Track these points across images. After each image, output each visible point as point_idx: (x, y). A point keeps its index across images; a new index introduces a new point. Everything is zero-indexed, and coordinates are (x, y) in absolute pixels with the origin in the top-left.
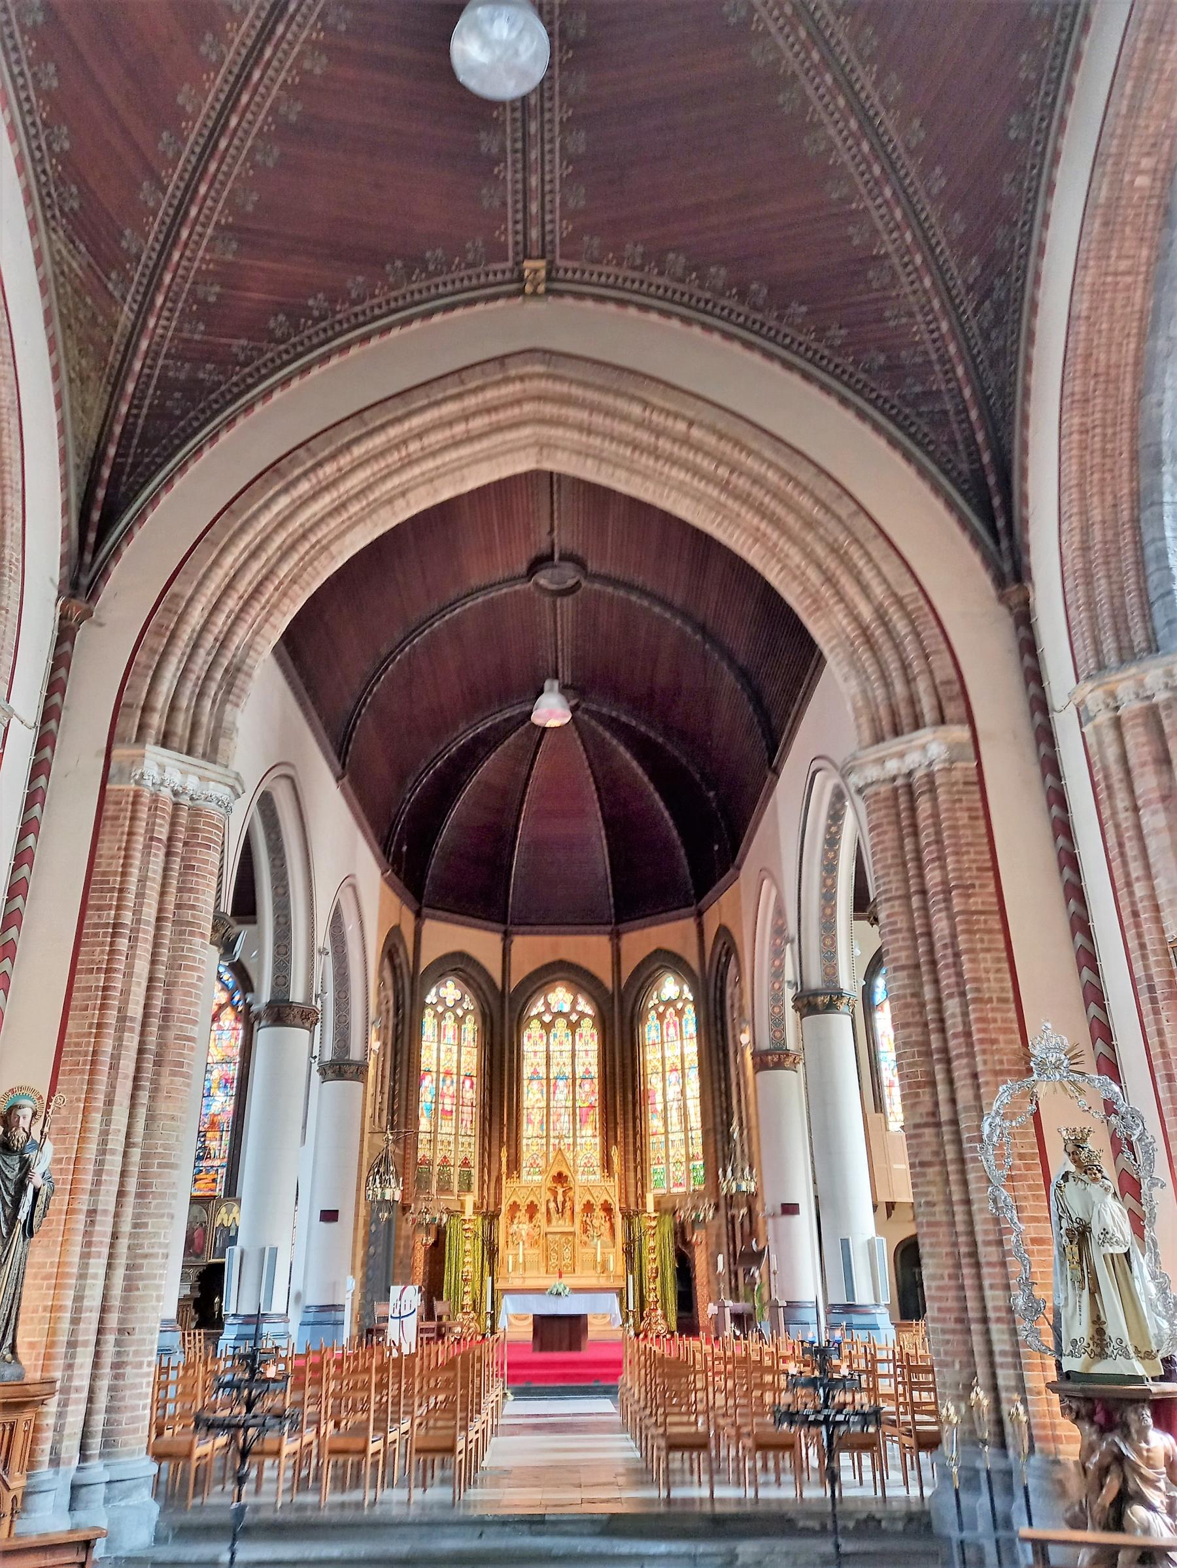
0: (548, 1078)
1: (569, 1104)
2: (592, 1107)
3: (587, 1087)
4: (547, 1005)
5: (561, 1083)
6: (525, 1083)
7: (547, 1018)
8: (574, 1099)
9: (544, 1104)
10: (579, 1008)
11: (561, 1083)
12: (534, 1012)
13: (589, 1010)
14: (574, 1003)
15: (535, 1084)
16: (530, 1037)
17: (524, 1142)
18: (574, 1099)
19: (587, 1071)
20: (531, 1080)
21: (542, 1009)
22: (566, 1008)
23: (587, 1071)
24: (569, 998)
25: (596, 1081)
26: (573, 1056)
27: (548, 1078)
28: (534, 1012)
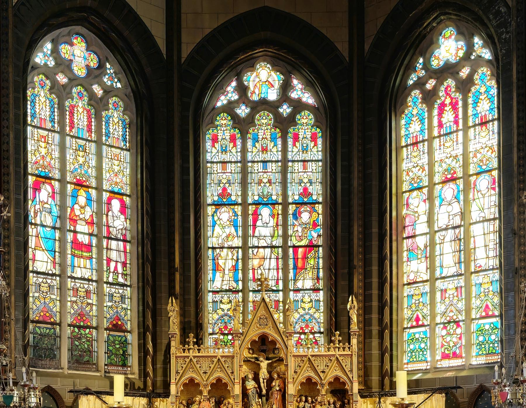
0: (245, 204)
1: (278, 242)
2: (311, 246)
3: (305, 217)
4: (242, 90)
5: (265, 212)
6: (210, 210)
7: (243, 111)
8: (285, 237)
9: (238, 242)
10: (294, 95)
11: (265, 212)
12: (222, 101)
13: (308, 98)
14: (286, 87)
15: (225, 215)
16: (215, 140)
17: (210, 297)
18: (285, 237)
19: (306, 192)
20: (218, 205)
21: (235, 97)
22: (273, 96)
23: (306, 192)
24: (277, 78)
25: (319, 208)
26: (284, 171)
27: (245, 204)
28: (222, 101)
